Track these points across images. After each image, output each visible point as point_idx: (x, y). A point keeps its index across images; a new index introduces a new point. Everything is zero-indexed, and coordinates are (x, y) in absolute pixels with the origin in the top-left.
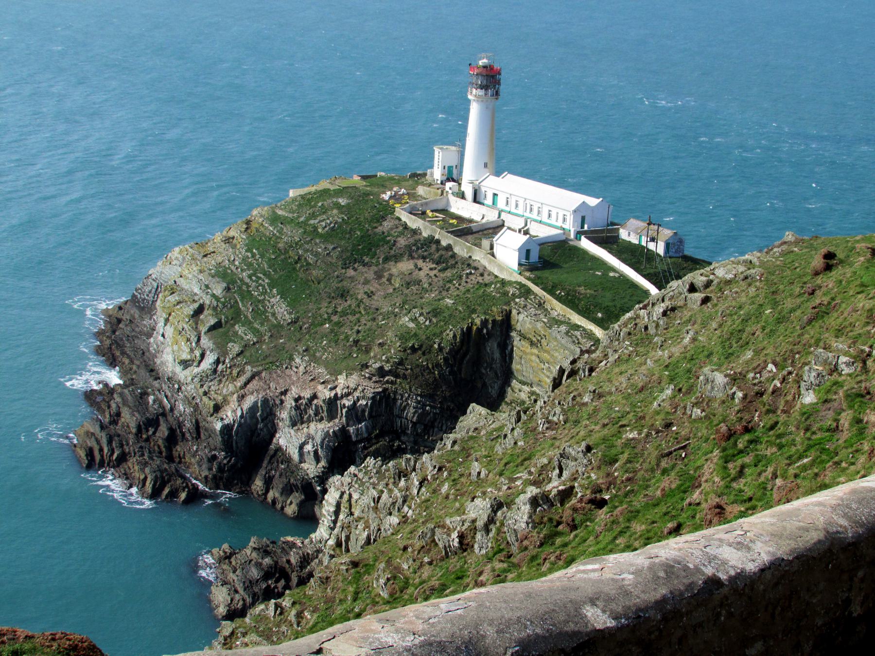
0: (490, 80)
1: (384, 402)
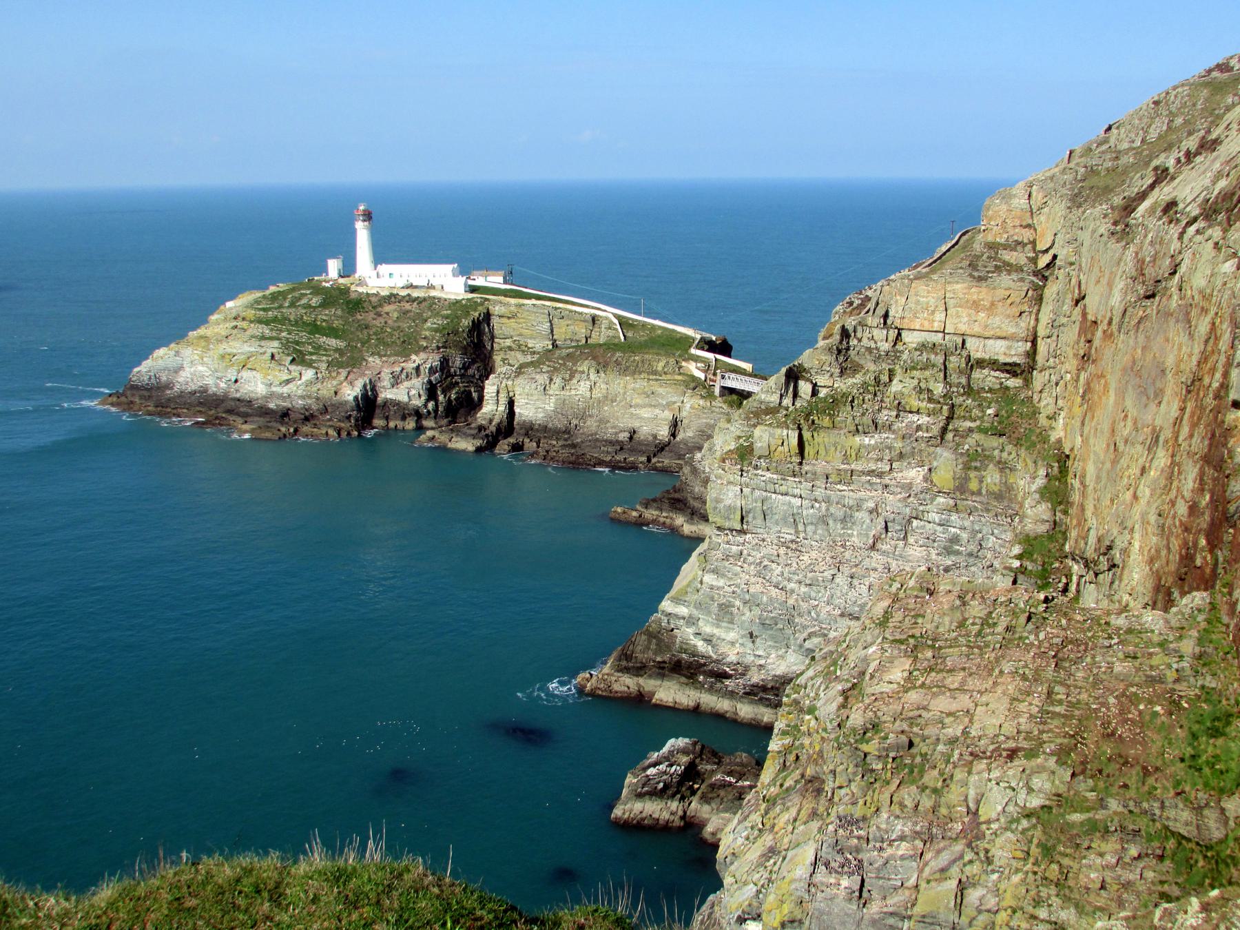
0: (368, 216)
1: (445, 362)
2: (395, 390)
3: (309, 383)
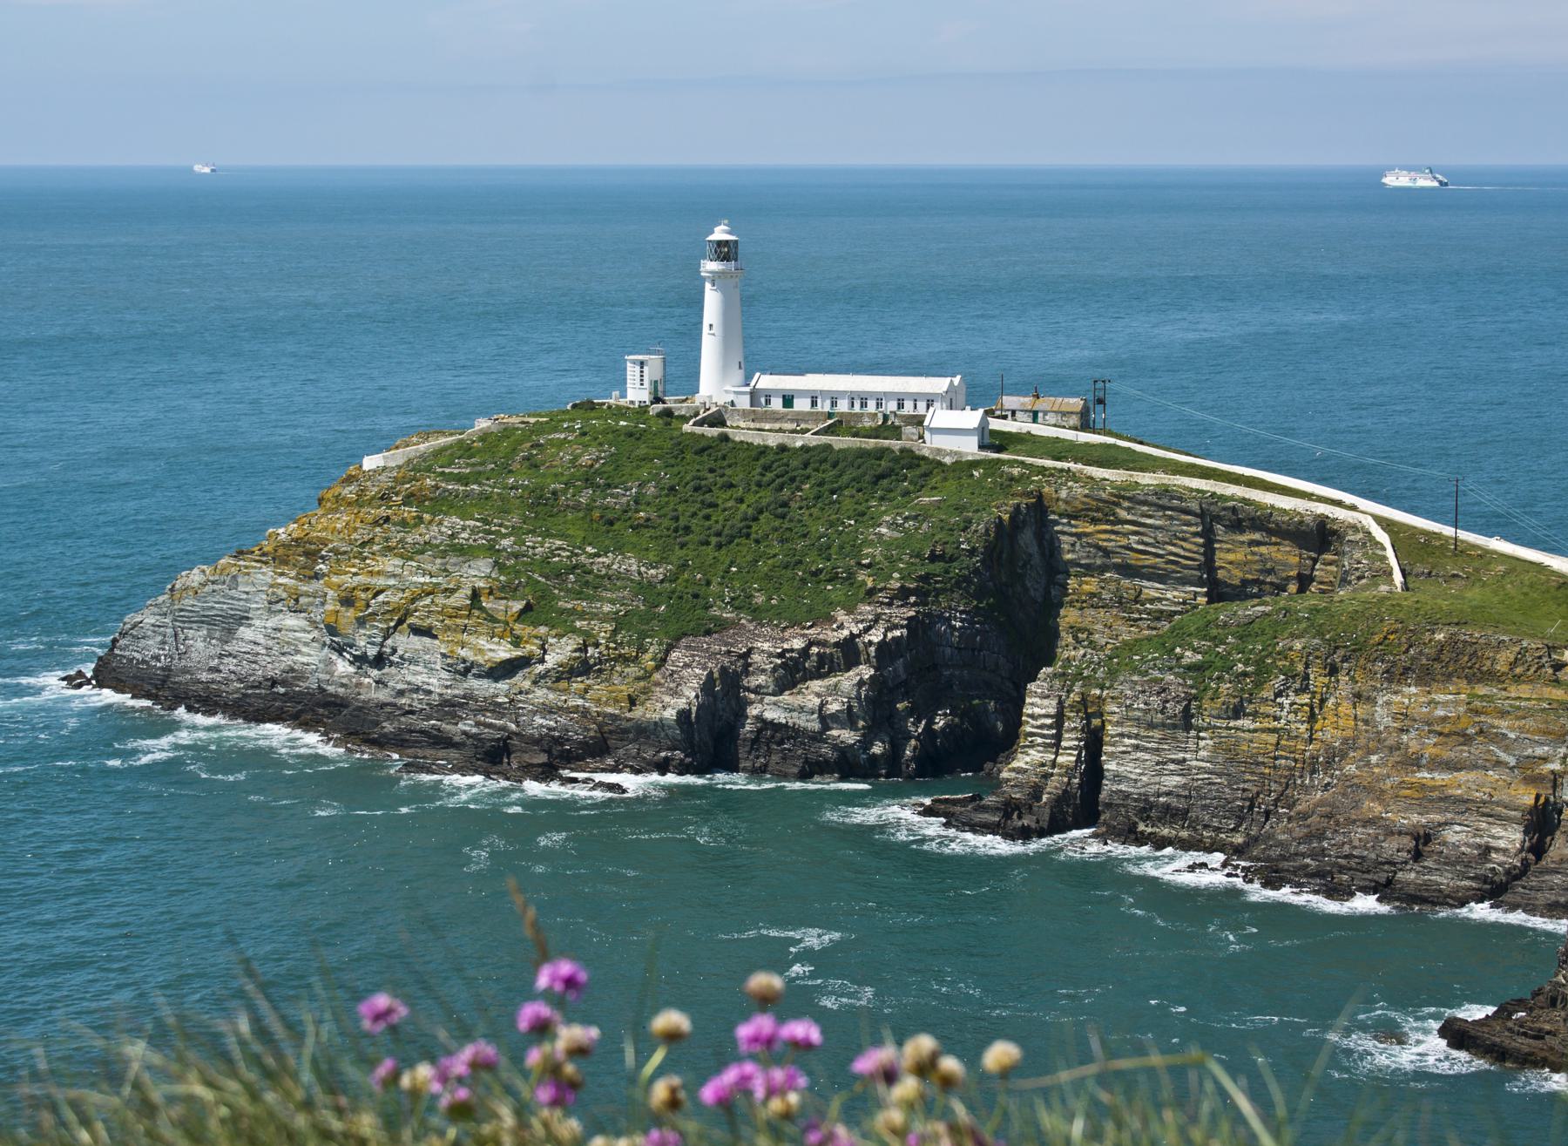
2: (786, 697)
3: (567, 673)
